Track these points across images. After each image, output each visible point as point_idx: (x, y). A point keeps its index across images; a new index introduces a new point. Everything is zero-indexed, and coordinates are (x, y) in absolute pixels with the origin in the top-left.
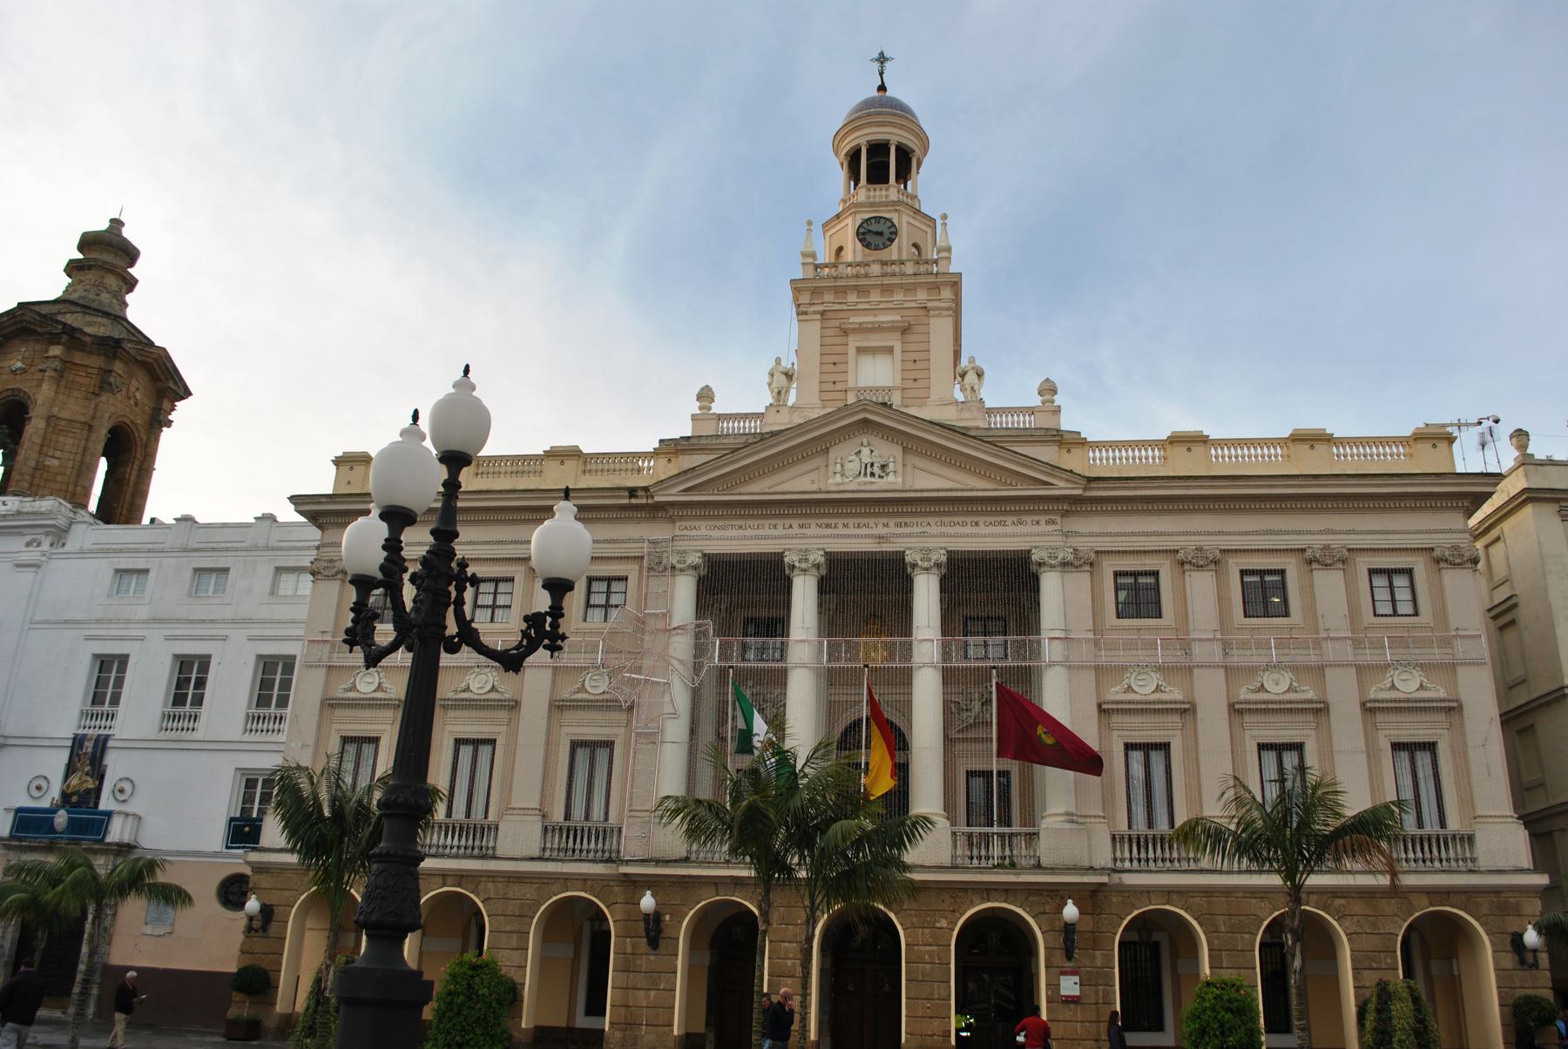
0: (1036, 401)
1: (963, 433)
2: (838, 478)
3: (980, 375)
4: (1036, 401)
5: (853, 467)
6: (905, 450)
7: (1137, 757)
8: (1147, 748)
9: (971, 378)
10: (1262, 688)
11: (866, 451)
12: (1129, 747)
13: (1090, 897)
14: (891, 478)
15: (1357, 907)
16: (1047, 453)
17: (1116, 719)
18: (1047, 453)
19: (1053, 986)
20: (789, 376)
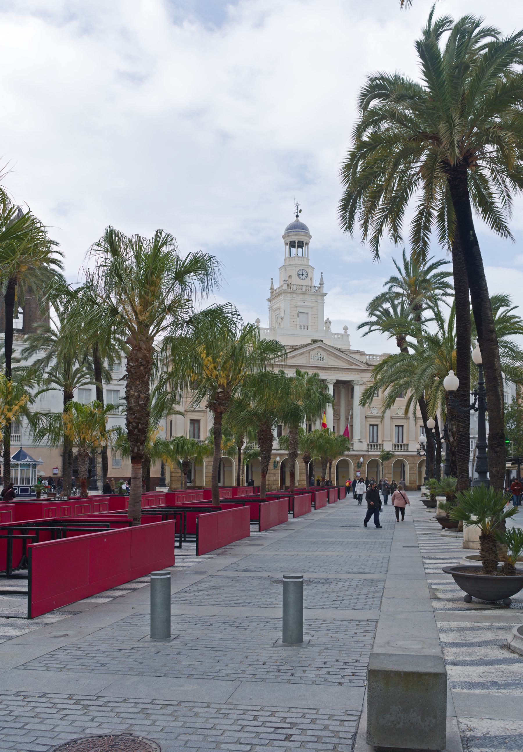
0: (342, 332)
1: (339, 350)
2: (313, 360)
3: (330, 323)
4: (342, 332)
5: (317, 358)
6: (327, 354)
7: (371, 427)
8: (373, 425)
9: (328, 323)
10: (397, 414)
11: (319, 354)
12: (370, 425)
13: (363, 456)
14: (325, 361)
15: (411, 459)
16: (357, 357)
17: (368, 419)
18: (357, 357)
19: (355, 474)
20: (282, 319)
